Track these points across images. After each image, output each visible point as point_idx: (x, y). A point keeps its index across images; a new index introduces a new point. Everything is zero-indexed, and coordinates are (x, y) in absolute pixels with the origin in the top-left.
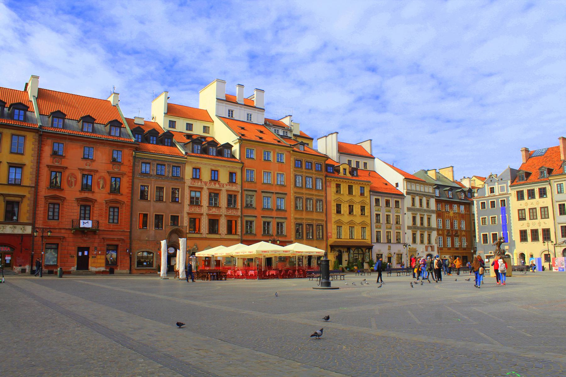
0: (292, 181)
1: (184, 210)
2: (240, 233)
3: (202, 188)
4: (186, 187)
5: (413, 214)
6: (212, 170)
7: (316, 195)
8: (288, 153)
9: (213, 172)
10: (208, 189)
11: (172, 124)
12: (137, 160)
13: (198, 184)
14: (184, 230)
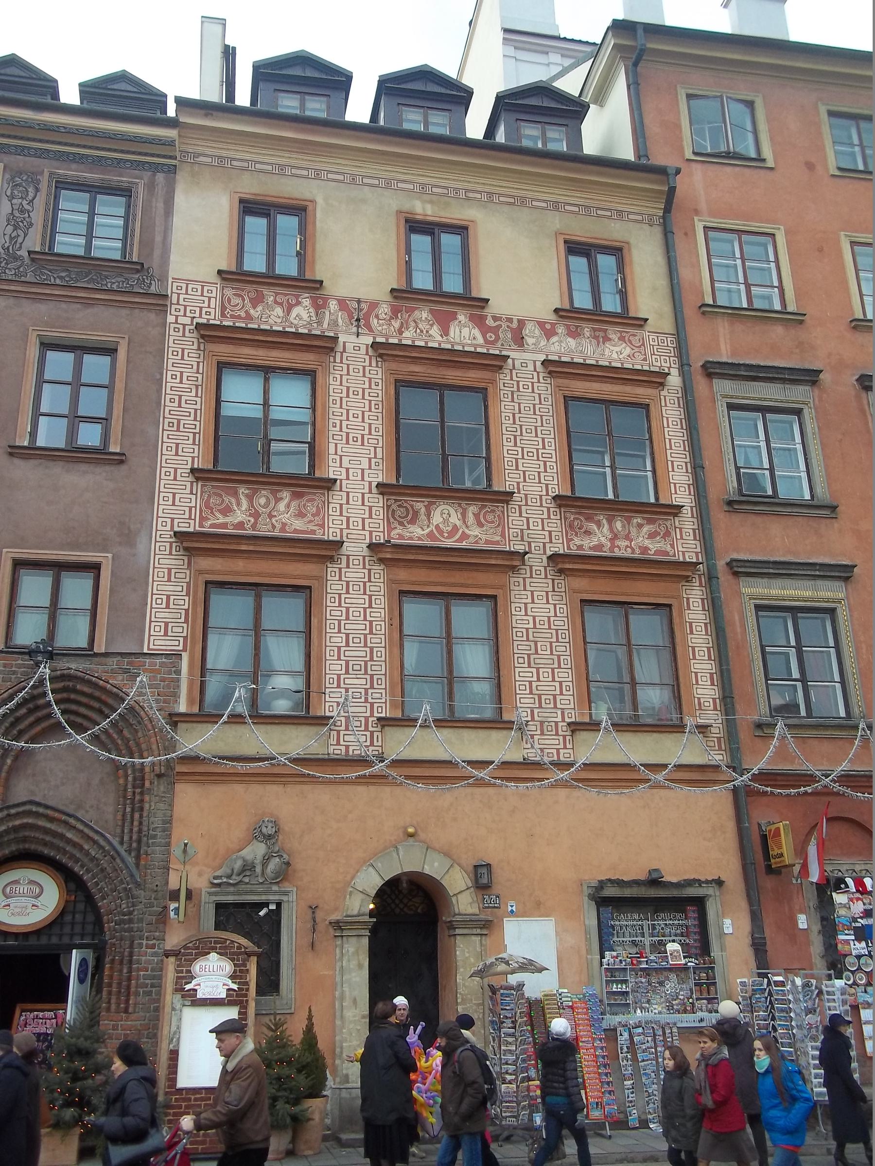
2: (713, 717)
3: (325, 346)
4: (172, 336)
10: (382, 351)
14: (139, 690)
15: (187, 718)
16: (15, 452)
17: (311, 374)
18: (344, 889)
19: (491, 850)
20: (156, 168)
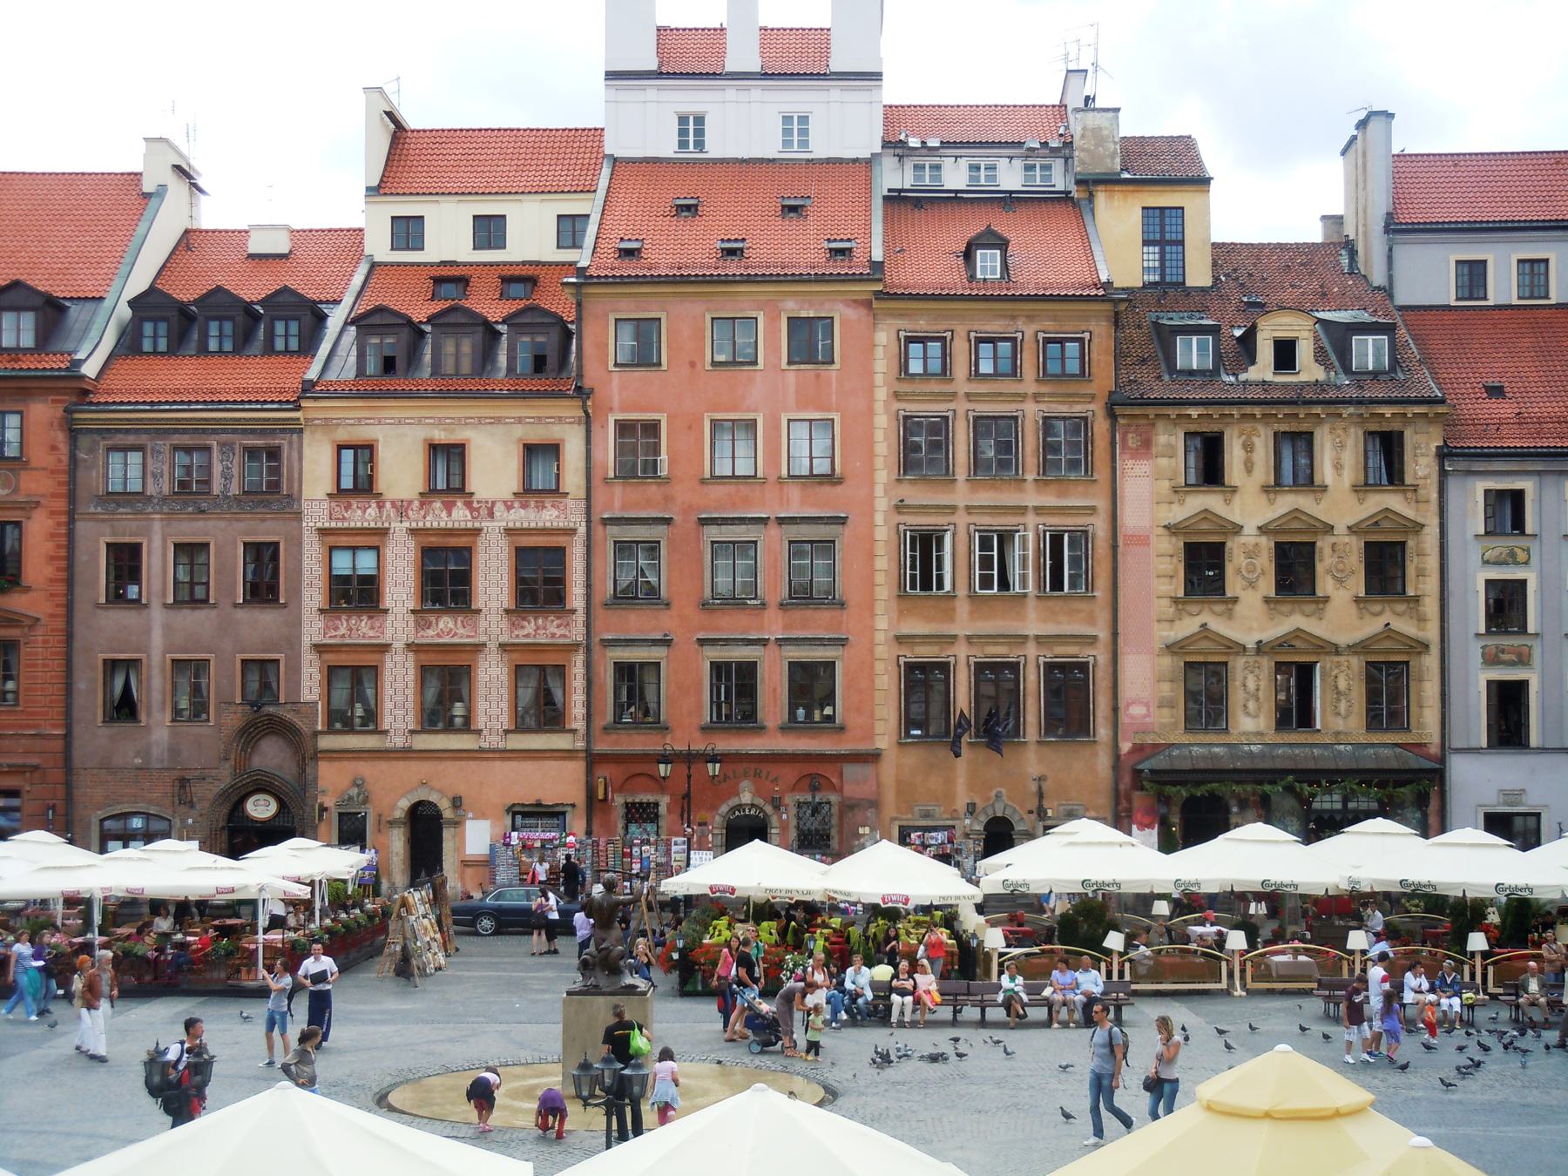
1: (299, 638)
3: (383, 532)
4: (306, 533)
7: (1039, 510)
8: (853, 314)
10: (413, 532)
11: (408, 231)
12: (84, 441)
13: (363, 515)
15: (322, 733)
16: (236, 605)
17: (377, 548)
18: (393, 807)
19: (461, 790)
20: (292, 431)
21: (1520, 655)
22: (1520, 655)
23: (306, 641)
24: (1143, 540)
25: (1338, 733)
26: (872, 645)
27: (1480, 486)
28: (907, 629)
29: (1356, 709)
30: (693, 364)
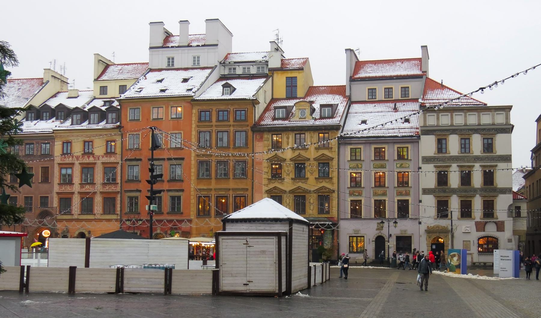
0: (194, 140)
2: (119, 213)
3: (73, 164)
5: (435, 167)
6: (85, 142)
9: (87, 144)
10: (80, 164)
14: (54, 212)
16: (39, 183)
17: (71, 168)
20: (52, 139)
21: (359, 193)
22: (359, 193)
23: (55, 191)
24: (260, 163)
25: (310, 215)
26: (190, 191)
27: (349, 147)
28: (199, 187)
29: (315, 208)
30: (148, 119)
